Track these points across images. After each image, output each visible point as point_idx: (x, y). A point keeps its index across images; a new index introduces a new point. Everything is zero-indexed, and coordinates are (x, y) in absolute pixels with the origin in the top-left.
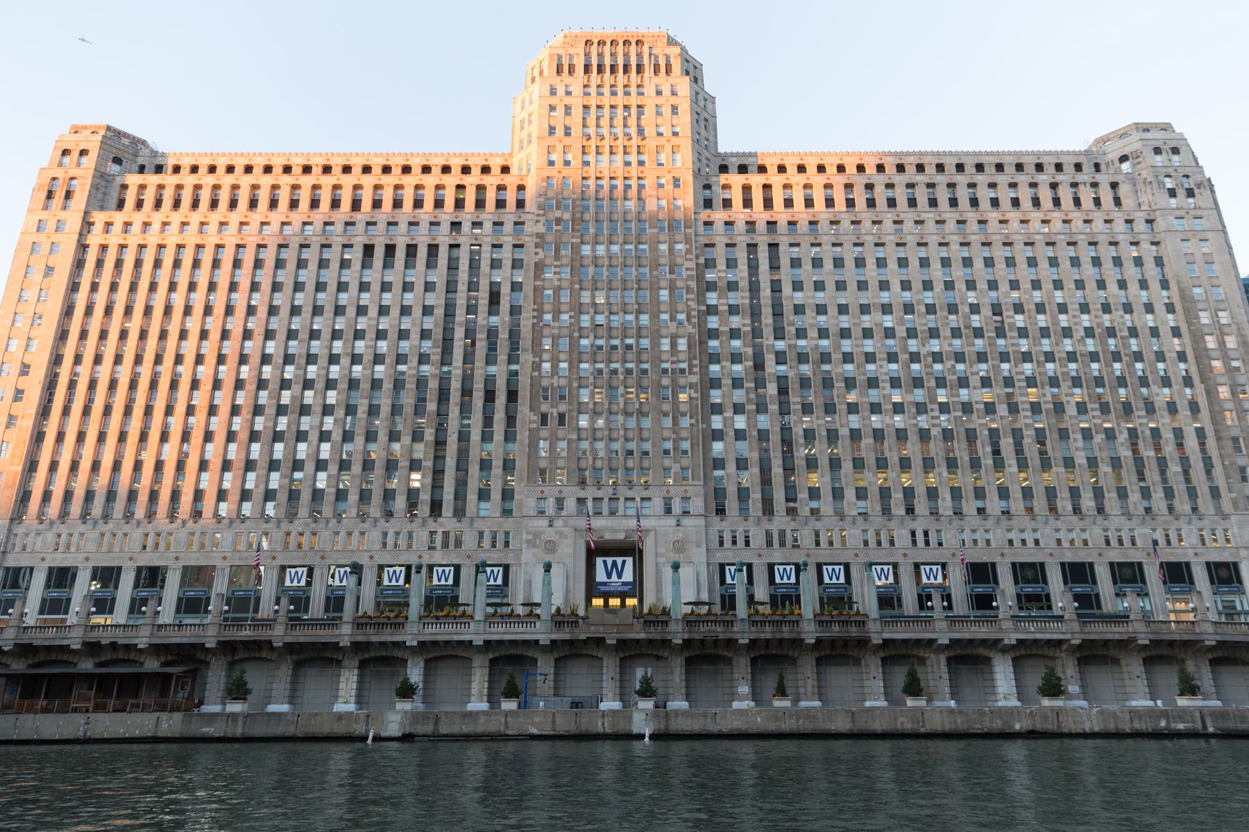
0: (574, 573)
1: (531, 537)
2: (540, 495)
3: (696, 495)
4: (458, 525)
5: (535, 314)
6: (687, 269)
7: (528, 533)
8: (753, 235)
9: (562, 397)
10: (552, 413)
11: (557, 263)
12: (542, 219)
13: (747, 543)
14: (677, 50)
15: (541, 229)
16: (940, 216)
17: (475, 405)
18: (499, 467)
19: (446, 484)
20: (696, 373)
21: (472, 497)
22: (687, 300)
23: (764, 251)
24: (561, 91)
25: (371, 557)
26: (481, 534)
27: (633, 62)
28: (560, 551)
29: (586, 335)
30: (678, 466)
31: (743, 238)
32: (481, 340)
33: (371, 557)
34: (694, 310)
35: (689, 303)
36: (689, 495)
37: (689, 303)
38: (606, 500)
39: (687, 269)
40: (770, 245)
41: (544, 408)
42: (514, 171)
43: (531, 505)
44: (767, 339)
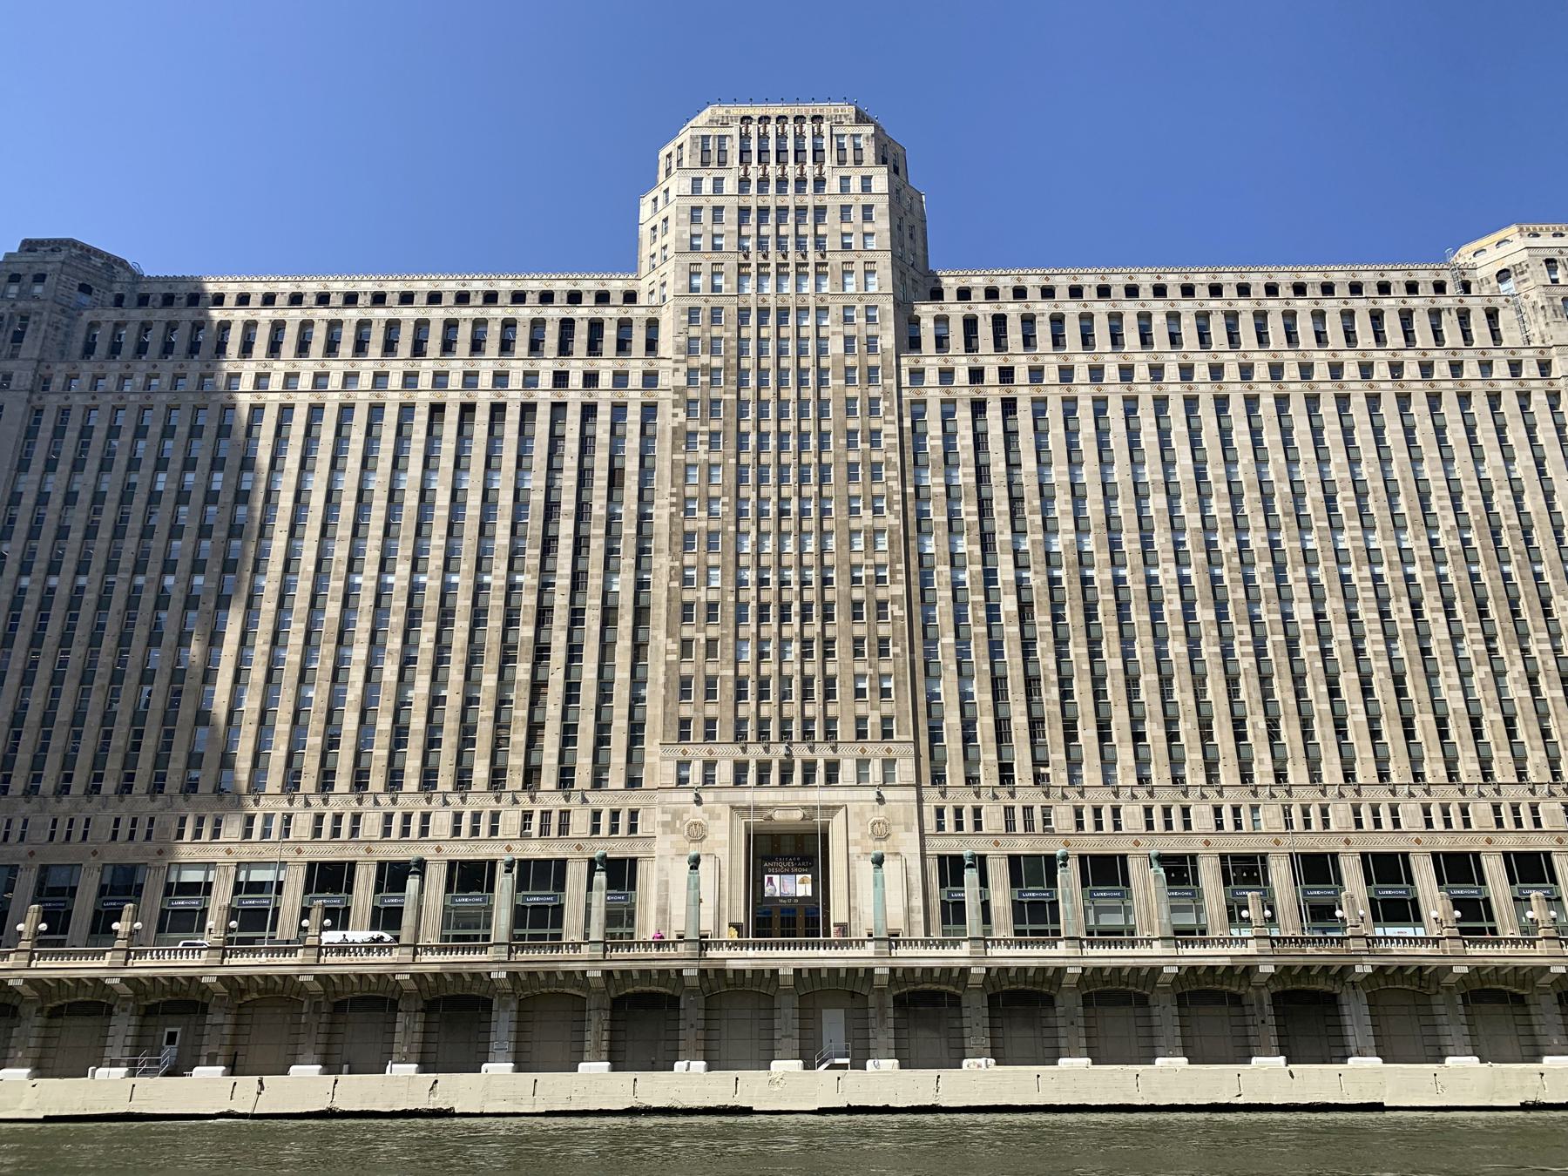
1: (668, 818)
3: (903, 757)
5: (674, 500)
6: (886, 436)
10: (698, 640)
11: (705, 429)
12: (683, 368)
13: (978, 826)
14: (870, 130)
16: (1245, 357)
18: (623, 717)
24: (707, 186)
25: (439, 850)
26: (596, 815)
27: (808, 146)
28: (709, 838)
32: (597, 537)
33: (439, 850)
35: (890, 483)
37: (890, 483)
38: (775, 765)
39: (886, 436)
41: (687, 632)
42: (642, 299)
43: (669, 773)
44: (1001, 533)
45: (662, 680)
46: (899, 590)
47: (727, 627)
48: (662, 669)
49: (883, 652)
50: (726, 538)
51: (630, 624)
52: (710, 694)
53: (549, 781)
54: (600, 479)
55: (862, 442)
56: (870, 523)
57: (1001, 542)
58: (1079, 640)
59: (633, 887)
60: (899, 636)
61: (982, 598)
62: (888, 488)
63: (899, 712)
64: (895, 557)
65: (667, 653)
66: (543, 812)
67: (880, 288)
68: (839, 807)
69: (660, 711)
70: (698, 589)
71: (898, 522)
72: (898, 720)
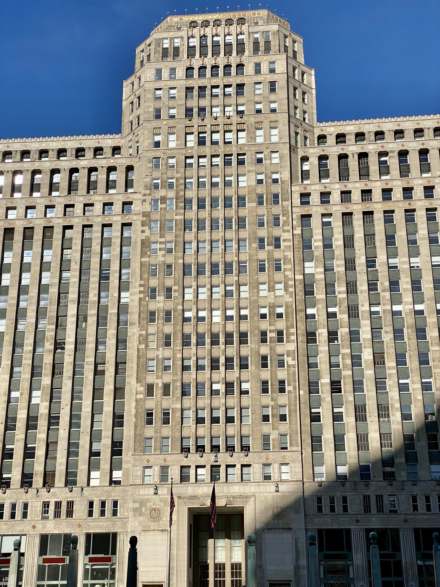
0: (178, 540)
1: (137, 505)
2: (146, 464)
3: (294, 461)
4: (69, 494)
5: (142, 289)
6: (284, 240)
7: (134, 502)
8: (348, 205)
9: (167, 368)
11: (162, 240)
15: (147, 208)
17: (86, 378)
19: (58, 456)
20: (293, 341)
21: (83, 467)
22: (284, 269)
23: (358, 220)
29: (189, 307)
30: (276, 432)
31: (338, 208)
34: (290, 279)
35: (287, 273)
36: (287, 461)
38: (208, 467)
39: (284, 240)
40: (365, 213)
41: (150, 379)
44: (362, 305)
45: (133, 411)
46: (292, 347)
47: (176, 374)
48: (134, 404)
49: (282, 390)
50: (176, 314)
51: (113, 374)
52: (166, 421)
53: (60, 481)
54: (94, 276)
55: (268, 245)
56: (272, 301)
57: (362, 312)
58: (415, 379)
59: (114, 553)
60: (292, 378)
61: (349, 351)
62: (285, 277)
63: (291, 431)
64: (289, 324)
65: (137, 394)
66: (56, 502)
67: (280, 139)
68: (251, 497)
69: (132, 433)
70: (157, 349)
71: (292, 300)
72: (290, 437)
